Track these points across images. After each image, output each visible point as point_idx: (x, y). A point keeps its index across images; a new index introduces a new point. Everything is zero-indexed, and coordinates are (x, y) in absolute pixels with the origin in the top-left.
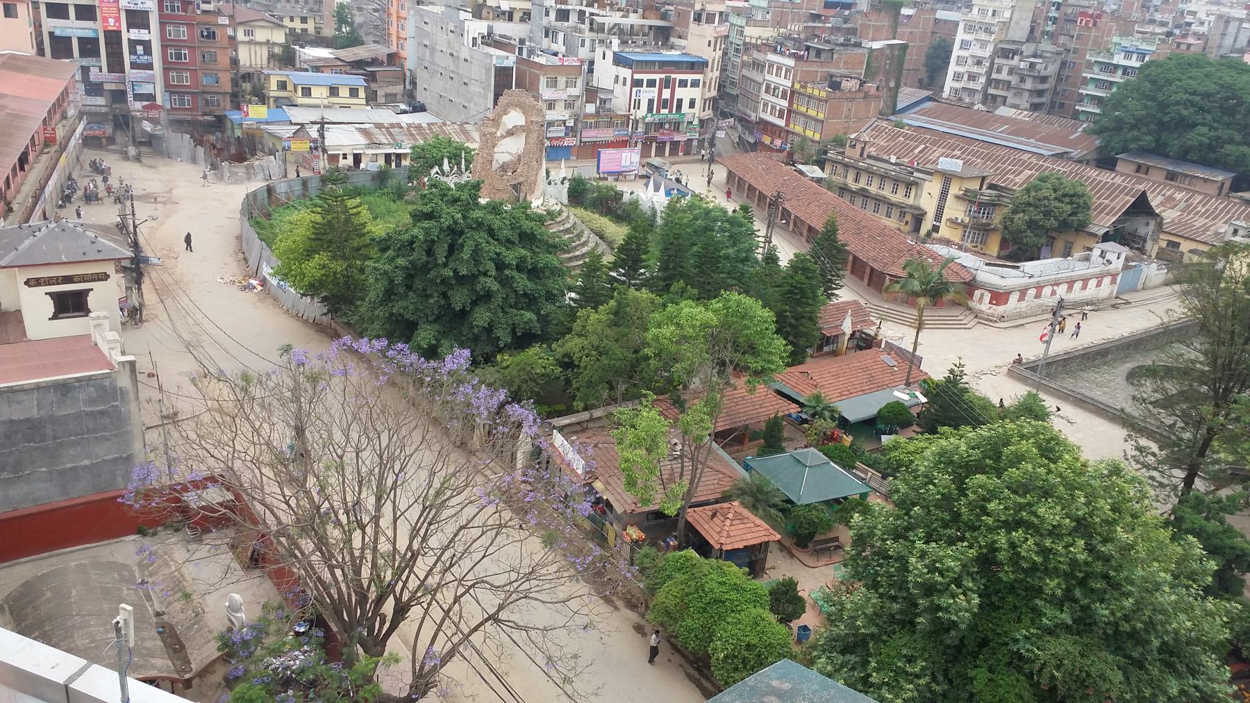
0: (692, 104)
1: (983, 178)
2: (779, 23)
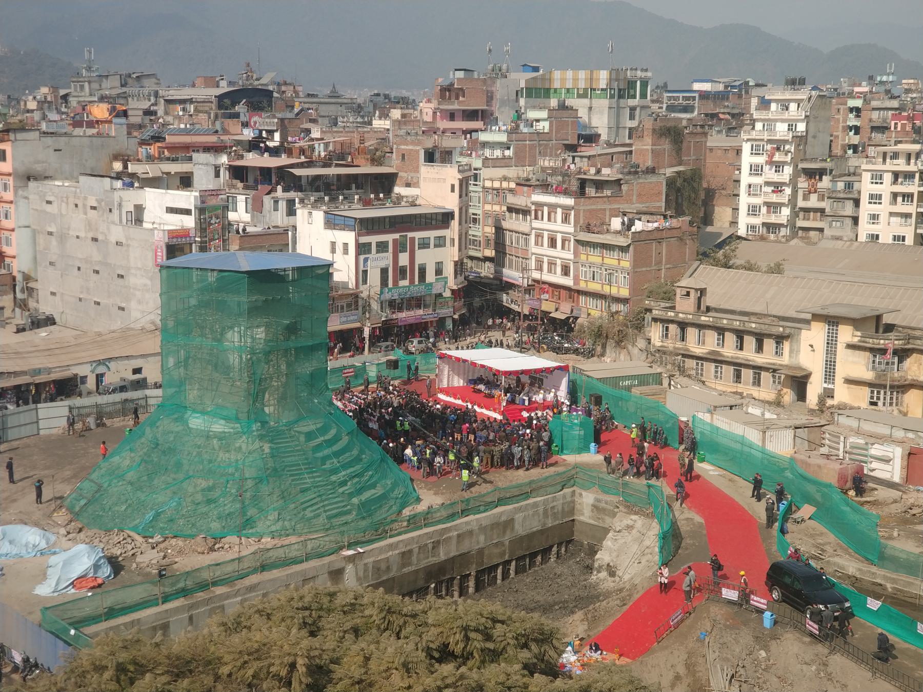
0: (439, 272)
1: (878, 318)
2: (519, 160)
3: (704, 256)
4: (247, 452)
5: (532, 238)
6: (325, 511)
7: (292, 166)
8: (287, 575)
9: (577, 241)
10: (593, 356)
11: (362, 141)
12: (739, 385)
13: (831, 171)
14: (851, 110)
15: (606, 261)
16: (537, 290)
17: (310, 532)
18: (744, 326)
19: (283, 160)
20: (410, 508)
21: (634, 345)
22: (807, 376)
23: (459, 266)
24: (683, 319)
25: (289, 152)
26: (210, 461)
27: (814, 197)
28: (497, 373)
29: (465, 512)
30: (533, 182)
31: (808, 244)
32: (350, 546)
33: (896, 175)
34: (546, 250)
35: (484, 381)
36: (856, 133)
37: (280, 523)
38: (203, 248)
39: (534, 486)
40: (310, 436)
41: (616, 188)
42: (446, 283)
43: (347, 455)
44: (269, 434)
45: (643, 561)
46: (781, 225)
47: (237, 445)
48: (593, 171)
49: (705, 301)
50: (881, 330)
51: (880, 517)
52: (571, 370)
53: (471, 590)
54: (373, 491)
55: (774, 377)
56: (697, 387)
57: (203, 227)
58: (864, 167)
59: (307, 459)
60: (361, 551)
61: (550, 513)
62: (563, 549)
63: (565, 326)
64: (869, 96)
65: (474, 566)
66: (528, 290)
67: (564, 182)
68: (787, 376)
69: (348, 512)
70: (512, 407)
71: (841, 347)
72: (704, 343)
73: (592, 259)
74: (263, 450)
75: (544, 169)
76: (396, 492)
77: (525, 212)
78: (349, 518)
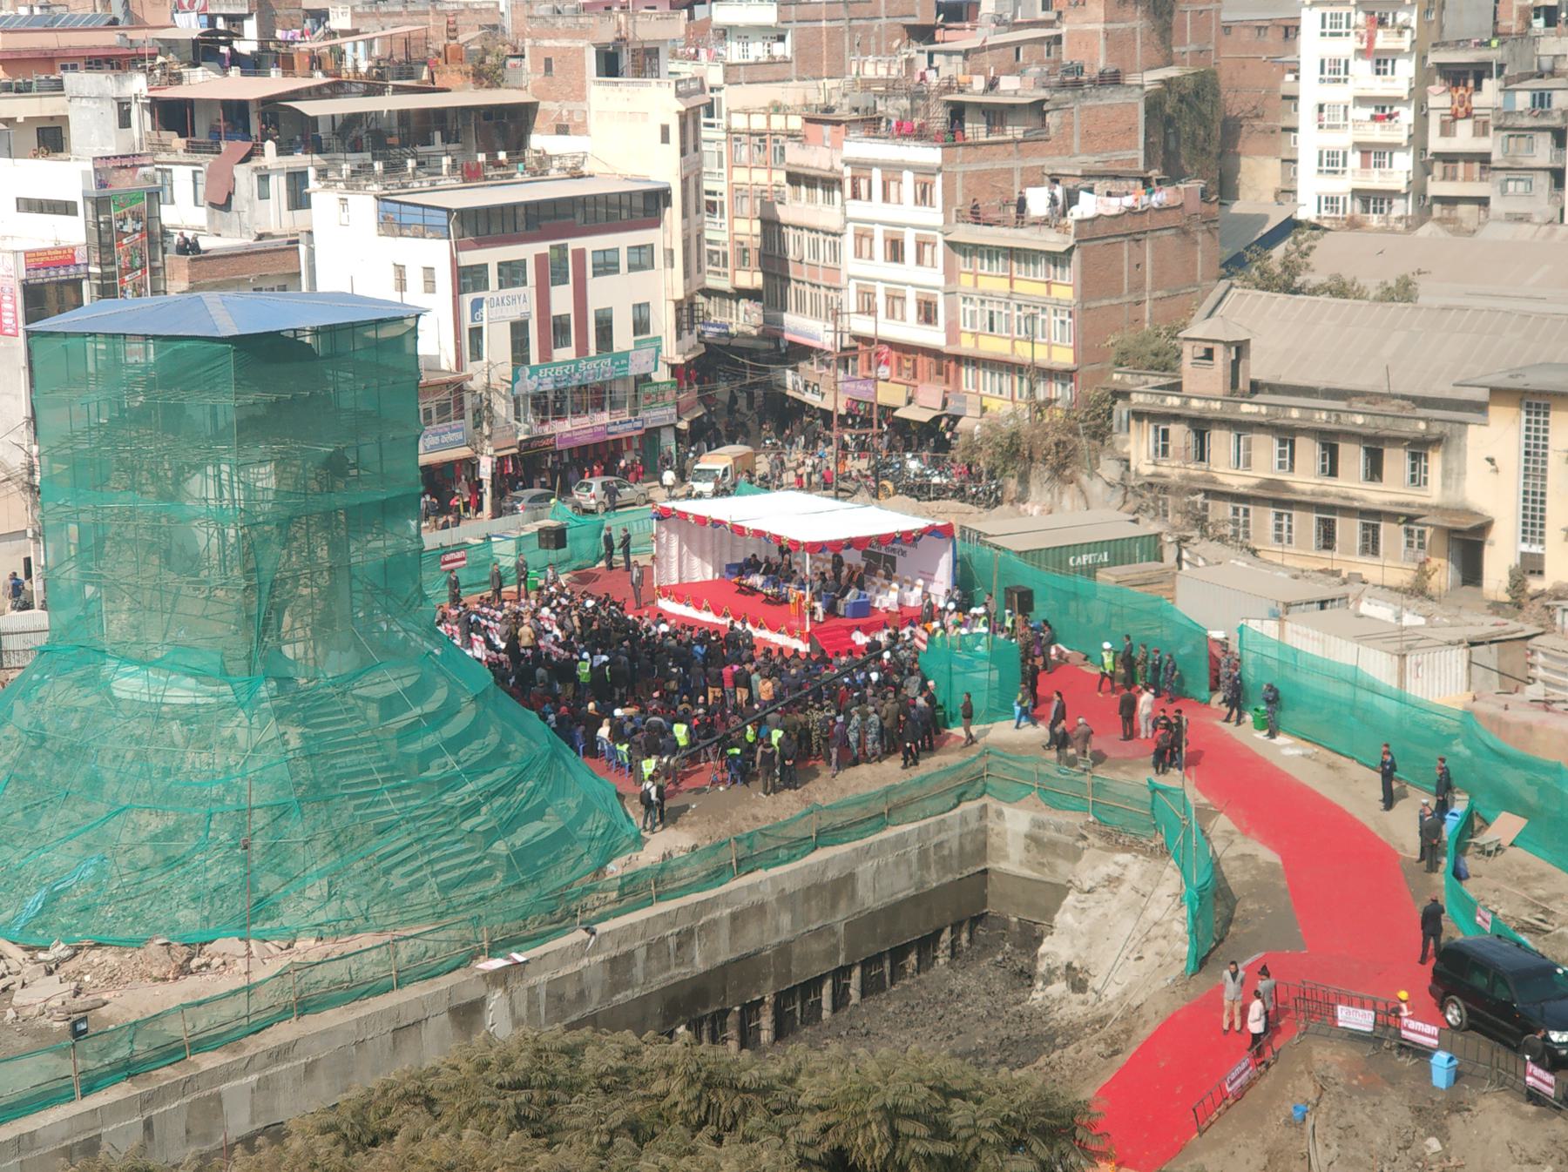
0: (641, 326)
2: (807, 65)
3: (1234, 265)
4: (250, 747)
6: (435, 874)
7: (297, 95)
8: (358, 1021)
9: (953, 245)
10: (998, 502)
12: (1327, 554)
13: (1501, 67)
15: (1019, 287)
17: (403, 923)
18: (1338, 421)
19: (274, 83)
20: (623, 859)
21: (1092, 474)
22: (1484, 528)
23: (687, 313)
24: (1200, 410)
25: (287, 64)
26: (167, 773)
27: (1464, 128)
28: (788, 548)
29: (745, 864)
30: (843, 113)
31: (1458, 231)
32: (493, 950)
34: (879, 268)
35: (767, 565)
37: (335, 904)
38: (107, 290)
39: (895, 799)
40: (389, 706)
41: (1034, 121)
42: (659, 350)
43: (475, 745)
44: (296, 704)
45: (1149, 954)
46: (1394, 194)
47: (227, 733)
48: (979, 83)
49: (1247, 369)
52: (957, 535)
53: (766, 1036)
54: (537, 826)
55: (1409, 533)
56: (1241, 562)
57: (104, 241)
59: (386, 758)
60: (520, 958)
61: (932, 857)
62: (965, 936)
63: (932, 436)
65: (771, 982)
66: (845, 358)
67: (914, 111)
68: (1438, 528)
69: (487, 874)
70: (833, 622)
72: (1248, 464)
73: (986, 284)
74: (286, 743)
75: (867, 85)
76: (587, 826)
77: (830, 184)
78: (488, 887)
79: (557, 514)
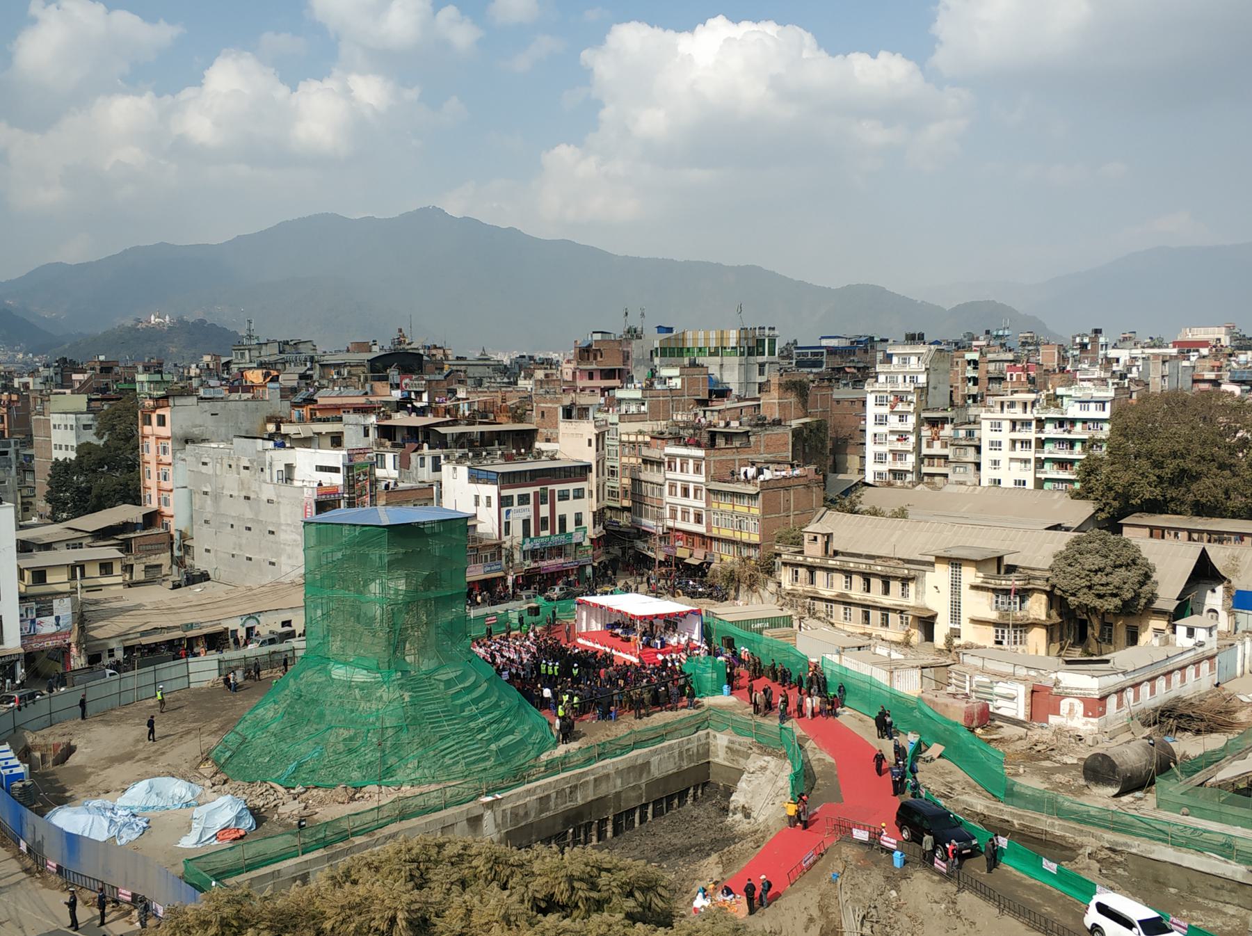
0: (578, 522)
3: (830, 503)
5: (666, 488)
9: (709, 490)
11: (504, 400)
14: (969, 362)
16: (672, 539)
23: (599, 516)
28: (633, 618)
29: (601, 756)
33: (1014, 423)
34: (679, 500)
36: (975, 384)
41: (745, 439)
50: (1002, 571)
51: (1005, 754)
54: (511, 737)
58: (983, 415)
63: (699, 571)
64: (985, 349)
66: (664, 537)
71: (965, 588)
77: (659, 463)
79: (540, 601)
